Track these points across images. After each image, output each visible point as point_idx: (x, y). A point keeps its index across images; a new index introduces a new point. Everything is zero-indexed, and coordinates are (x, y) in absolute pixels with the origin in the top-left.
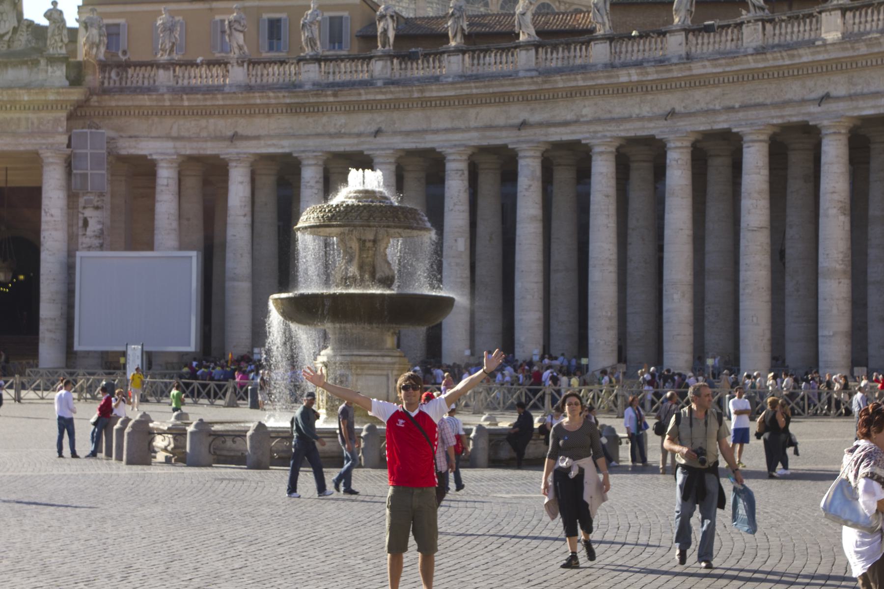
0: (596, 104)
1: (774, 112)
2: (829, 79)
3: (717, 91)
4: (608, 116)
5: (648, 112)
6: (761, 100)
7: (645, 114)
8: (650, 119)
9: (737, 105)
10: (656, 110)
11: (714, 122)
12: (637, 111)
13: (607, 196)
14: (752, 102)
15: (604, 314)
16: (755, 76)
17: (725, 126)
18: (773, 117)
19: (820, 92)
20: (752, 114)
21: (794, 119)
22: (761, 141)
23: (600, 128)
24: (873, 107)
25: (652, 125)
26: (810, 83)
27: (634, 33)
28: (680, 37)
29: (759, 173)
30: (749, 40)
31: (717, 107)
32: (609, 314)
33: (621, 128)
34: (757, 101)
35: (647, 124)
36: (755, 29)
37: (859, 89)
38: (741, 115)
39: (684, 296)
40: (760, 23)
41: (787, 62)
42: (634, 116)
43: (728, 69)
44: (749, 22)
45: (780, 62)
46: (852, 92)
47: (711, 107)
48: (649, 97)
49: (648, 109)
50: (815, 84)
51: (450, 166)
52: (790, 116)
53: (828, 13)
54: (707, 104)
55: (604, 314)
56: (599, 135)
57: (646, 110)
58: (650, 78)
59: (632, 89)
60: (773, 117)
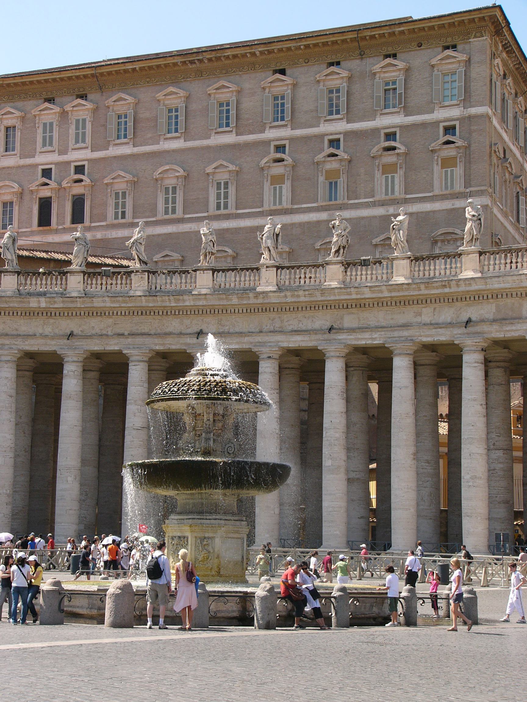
0: (4, 323)
1: (156, 341)
2: (202, 320)
3: (110, 321)
4: (15, 333)
5: (50, 333)
6: (146, 330)
7: (47, 333)
8: (53, 338)
9: (126, 333)
10: (57, 331)
11: (107, 344)
12: (41, 331)
13: (11, 396)
14: (139, 332)
15: (4, 491)
16: (144, 312)
17: (117, 348)
18: (156, 345)
19: (196, 329)
20: (139, 340)
21: (174, 347)
22: (143, 361)
23: (7, 342)
24: (238, 343)
25: (53, 342)
26: (187, 321)
27: (41, 270)
28: (80, 277)
29: (143, 386)
30: (136, 285)
31: (110, 333)
32: (8, 492)
33: (27, 343)
34: (143, 331)
35: (49, 342)
36: (142, 278)
37: (226, 329)
38: (130, 340)
39: (75, 479)
40: (147, 274)
41: (173, 304)
42: (38, 334)
43: (123, 305)
44: (137, 271)
45: (168, 304)
46: (221, 330)
47: (105, 332)
48: (52, 321)
49: (50, 330)
50: (191, 323)
51: (466, 358)
52: (170, 344)
53: (202, 272)
54: (101, 330)
55: (4, 491)
56: (6, 347)
57: (48, 330)
58: (56, 306)
59: (38, 313)
60: (156, 345)
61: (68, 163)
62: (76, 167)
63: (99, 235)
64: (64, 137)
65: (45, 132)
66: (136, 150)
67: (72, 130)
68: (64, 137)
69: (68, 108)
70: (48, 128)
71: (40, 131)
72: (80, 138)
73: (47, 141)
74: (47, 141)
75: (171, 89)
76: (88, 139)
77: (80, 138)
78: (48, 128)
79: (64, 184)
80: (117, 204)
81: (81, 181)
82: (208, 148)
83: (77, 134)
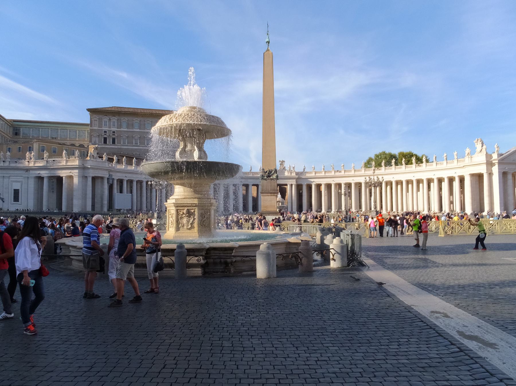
61: (111, 130)
62: (113, 132)
63: (119, 147)
64: (110, 125)
65: (105, 123)
66: (128, 130)
67: (112, 123)
68: (110, 125)
69: (111, 119)
70: (105, 122)
71: (103, 123)
72: (114, 125)
73: (105, 125)
74: (105, 125)
75: (136, 119)
76: (116, 126)
77: (114, 125)
78: (105, 122)
79: (111, 135)
80: (123, 141)
81: (115, 135)
82: (145, 132)
83: (113, 124)
